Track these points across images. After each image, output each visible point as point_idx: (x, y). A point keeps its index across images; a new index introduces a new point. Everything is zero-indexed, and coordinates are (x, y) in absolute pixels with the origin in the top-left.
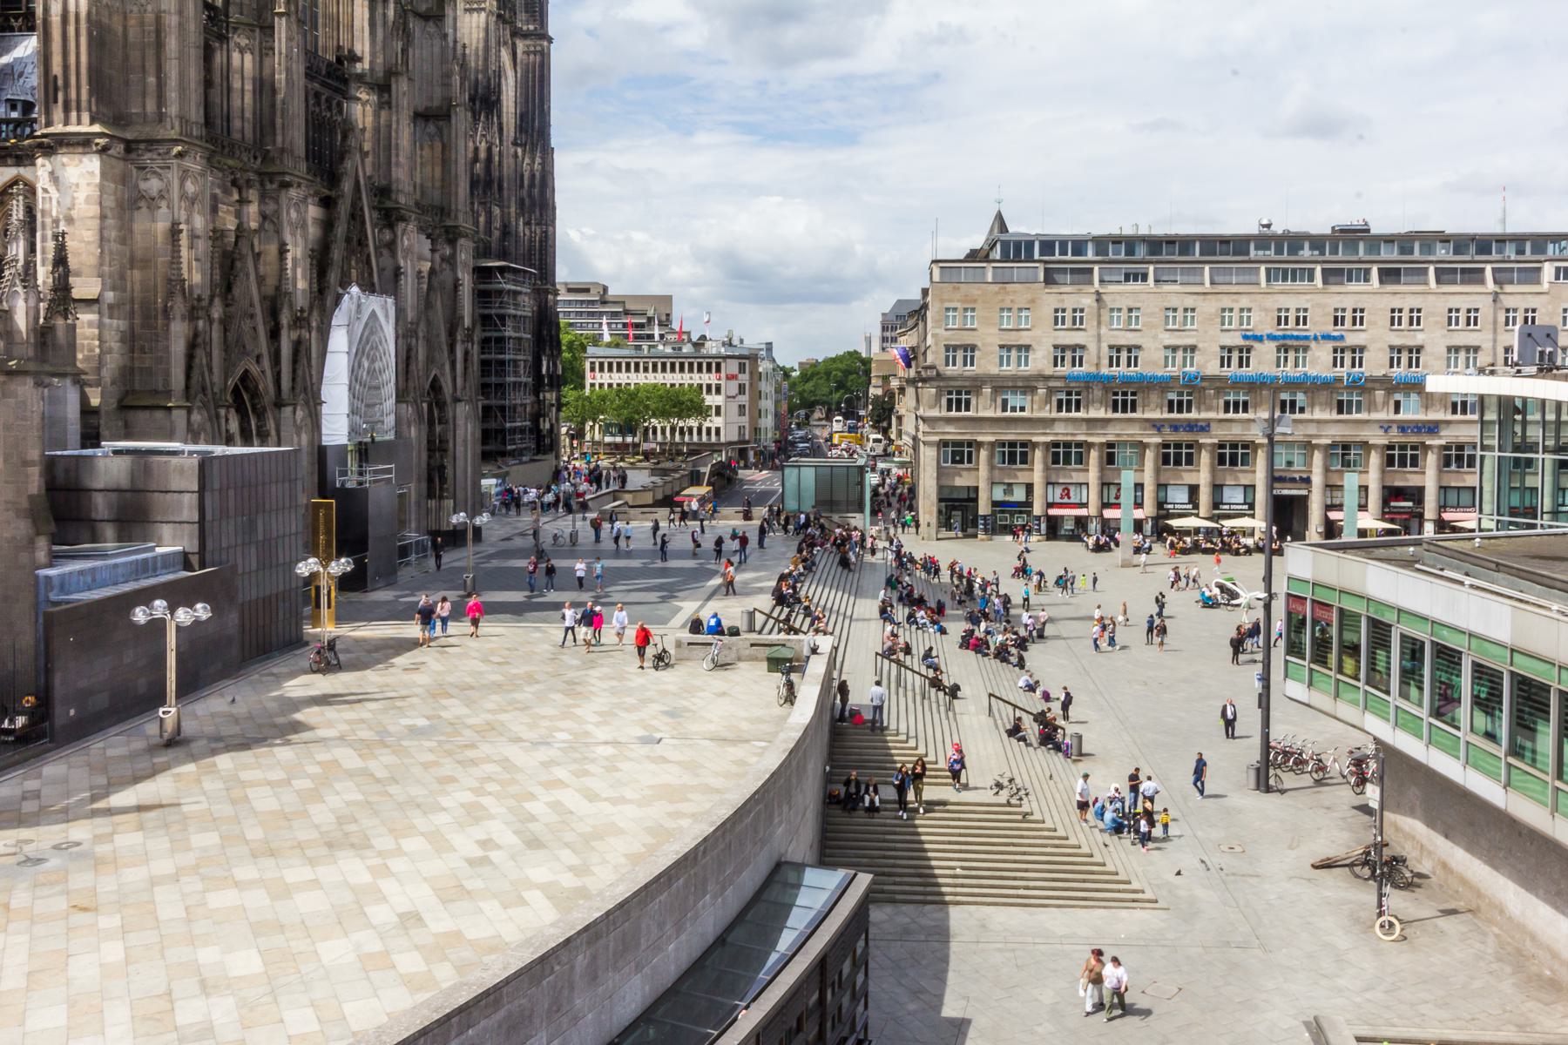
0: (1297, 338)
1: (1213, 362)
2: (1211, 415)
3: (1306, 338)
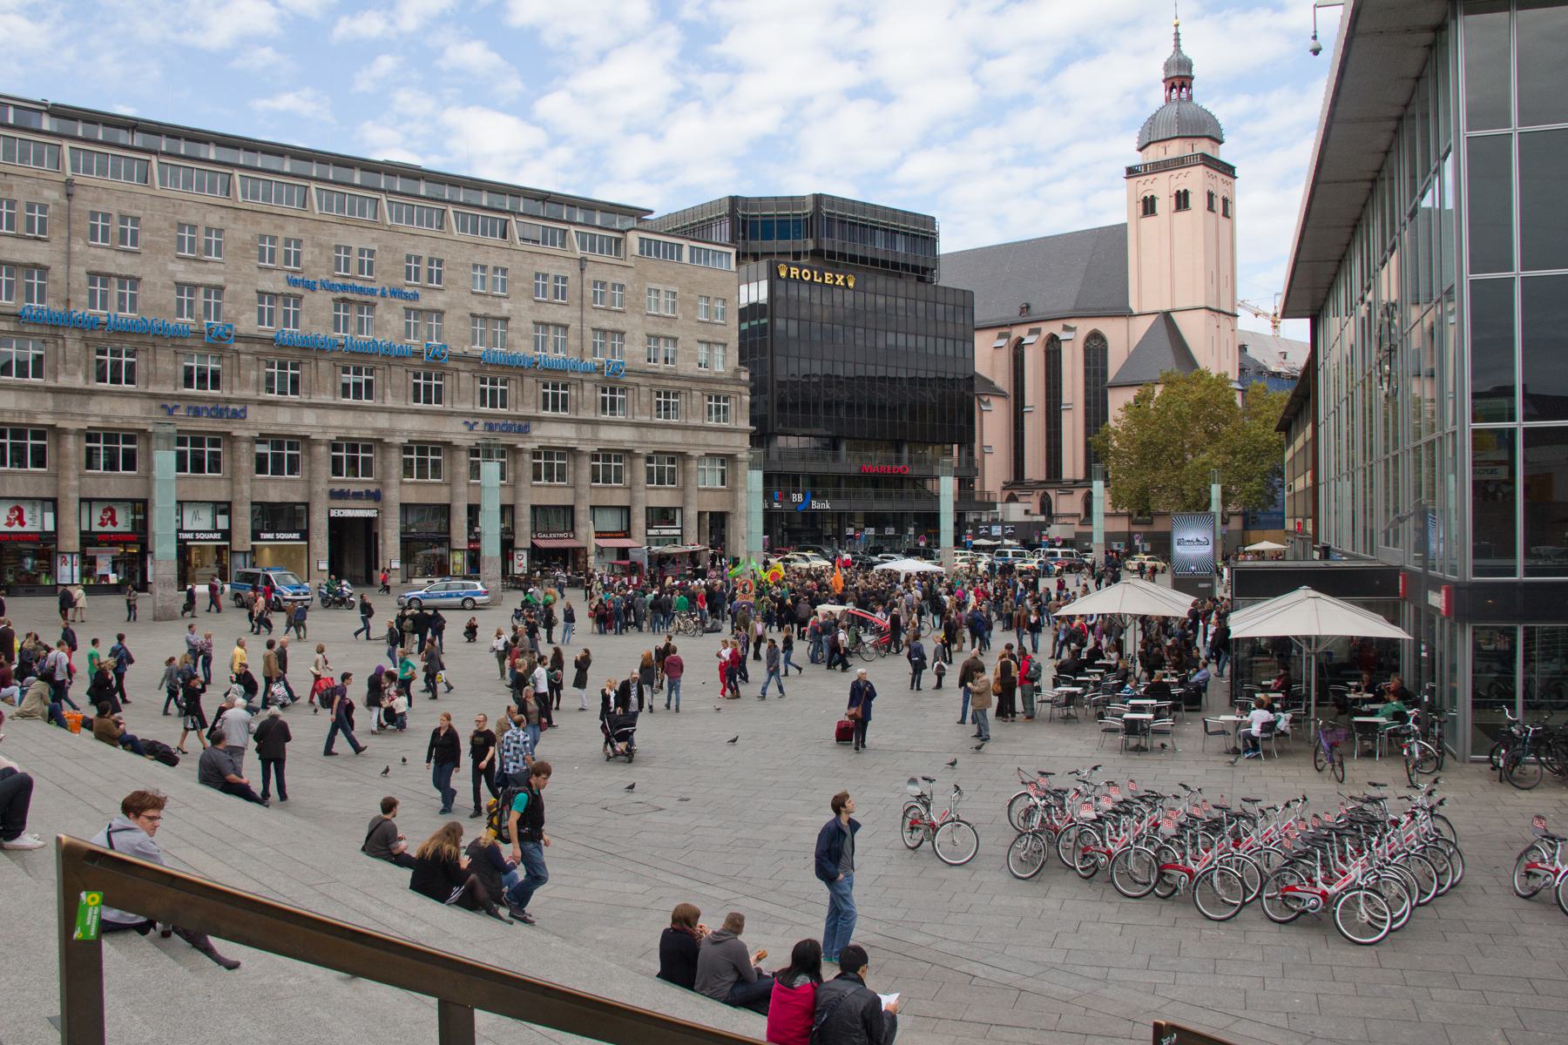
0: (361, 291)
1: (247, 315)
2: (249, 393)
3: (372, 292)
